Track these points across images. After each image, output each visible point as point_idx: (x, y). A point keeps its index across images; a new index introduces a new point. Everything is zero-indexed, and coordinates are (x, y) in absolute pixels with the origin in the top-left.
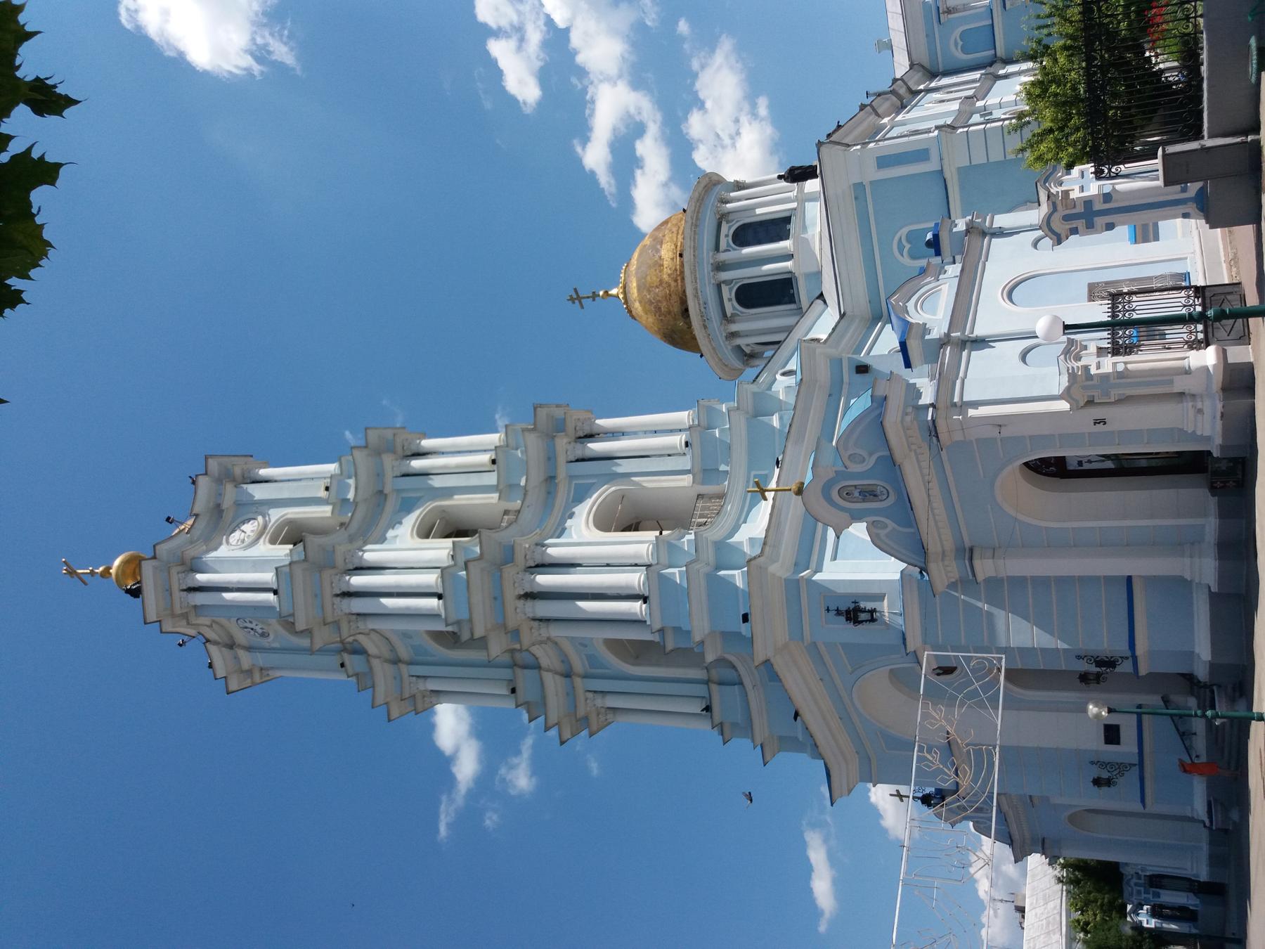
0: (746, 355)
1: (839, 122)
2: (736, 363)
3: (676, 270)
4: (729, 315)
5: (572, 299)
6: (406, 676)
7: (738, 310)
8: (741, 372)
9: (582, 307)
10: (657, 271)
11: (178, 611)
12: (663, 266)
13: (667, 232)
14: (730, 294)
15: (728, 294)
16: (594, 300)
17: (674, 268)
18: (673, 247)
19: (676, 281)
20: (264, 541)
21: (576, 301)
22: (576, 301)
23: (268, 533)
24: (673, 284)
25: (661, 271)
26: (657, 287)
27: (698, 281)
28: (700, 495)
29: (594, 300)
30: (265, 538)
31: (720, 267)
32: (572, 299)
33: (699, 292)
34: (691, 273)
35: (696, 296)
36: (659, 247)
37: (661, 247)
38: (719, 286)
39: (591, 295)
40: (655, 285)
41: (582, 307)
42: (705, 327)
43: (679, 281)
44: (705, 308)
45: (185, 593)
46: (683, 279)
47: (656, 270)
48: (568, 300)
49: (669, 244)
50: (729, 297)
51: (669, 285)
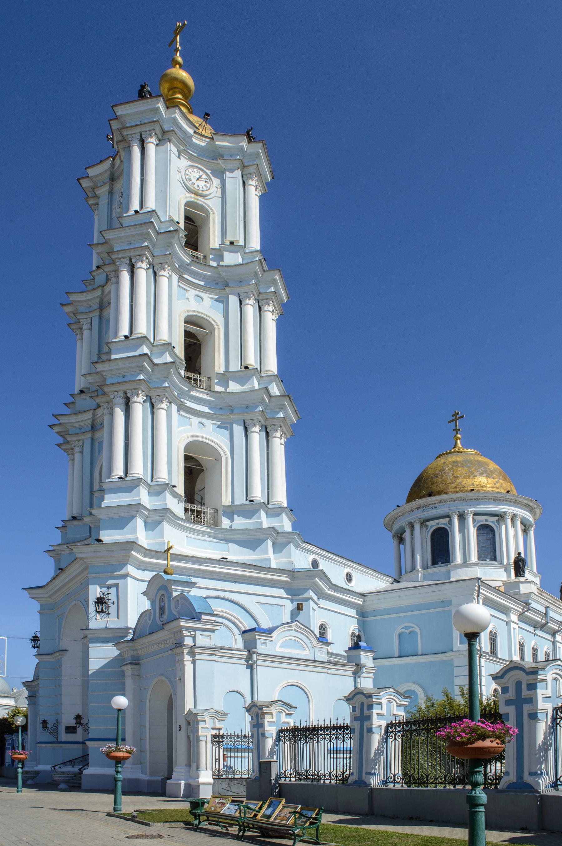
3: (464, 487)
5: (455, 414)
6: (91, 315)
7: (430, 529)
10: (465, 475)
11: (125, 133)
12: (469, 478)
13: (497, 480)
14: (441, 524)
15: (442, 523)
17: (465, 485)
18: (483, 485)
19: (456, 487)
20: (187, 197)
21: (454, 418)
22: (454, 418)
23: (196, 199)
24: (453, 485)
25: (465, 477)
26: (453, 474)
27: (453, 502)
30: (192, 197)
32: (455, 414)
33: (444, 503)
34: (458, 498)
35: (441, 501)
36: (485, 475)
40: (455, 473)
42: (418, 508)
43: (455, 490)
44: (432, 508)
45: (139, 137)
46: (457, 492)
47: (466, 473)
49: (486, 482)
50: (440, 523)
51: (453, 483)
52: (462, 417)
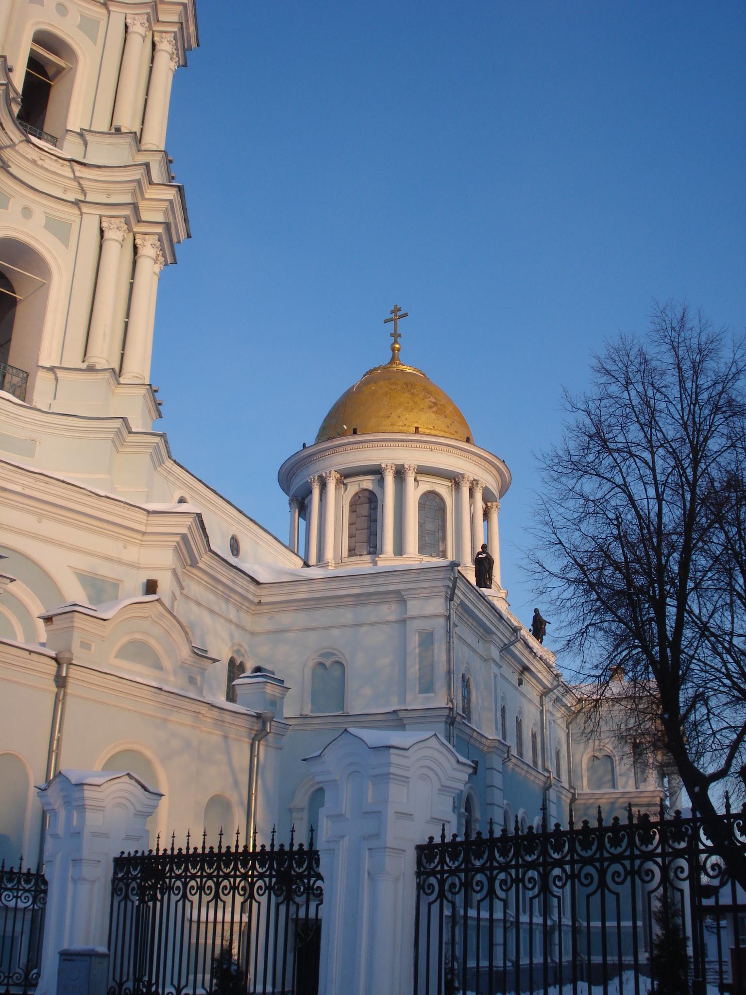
0: (303, 499)
1: (549, 623)
2: (297, 483)
4: (346, 481)
5: (397, 310)
8: (286, 490)
9: (386, 321)
16: (392, 335)
28: (28, 375)
29: (392, 335)
31: (400, 474)
32: (397, 310)
37: (432, 412)
38: (377, 472)
39: (398, 333)
41: (386, 321)
48: (396, 306)
51: (388, 417)
52: (406, 315)
